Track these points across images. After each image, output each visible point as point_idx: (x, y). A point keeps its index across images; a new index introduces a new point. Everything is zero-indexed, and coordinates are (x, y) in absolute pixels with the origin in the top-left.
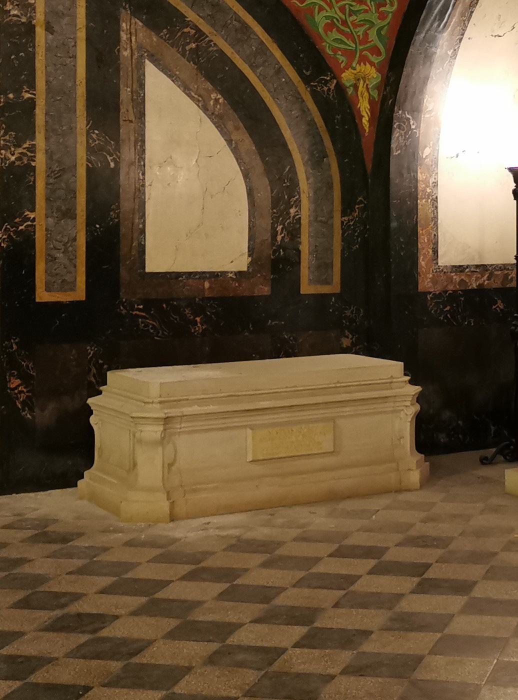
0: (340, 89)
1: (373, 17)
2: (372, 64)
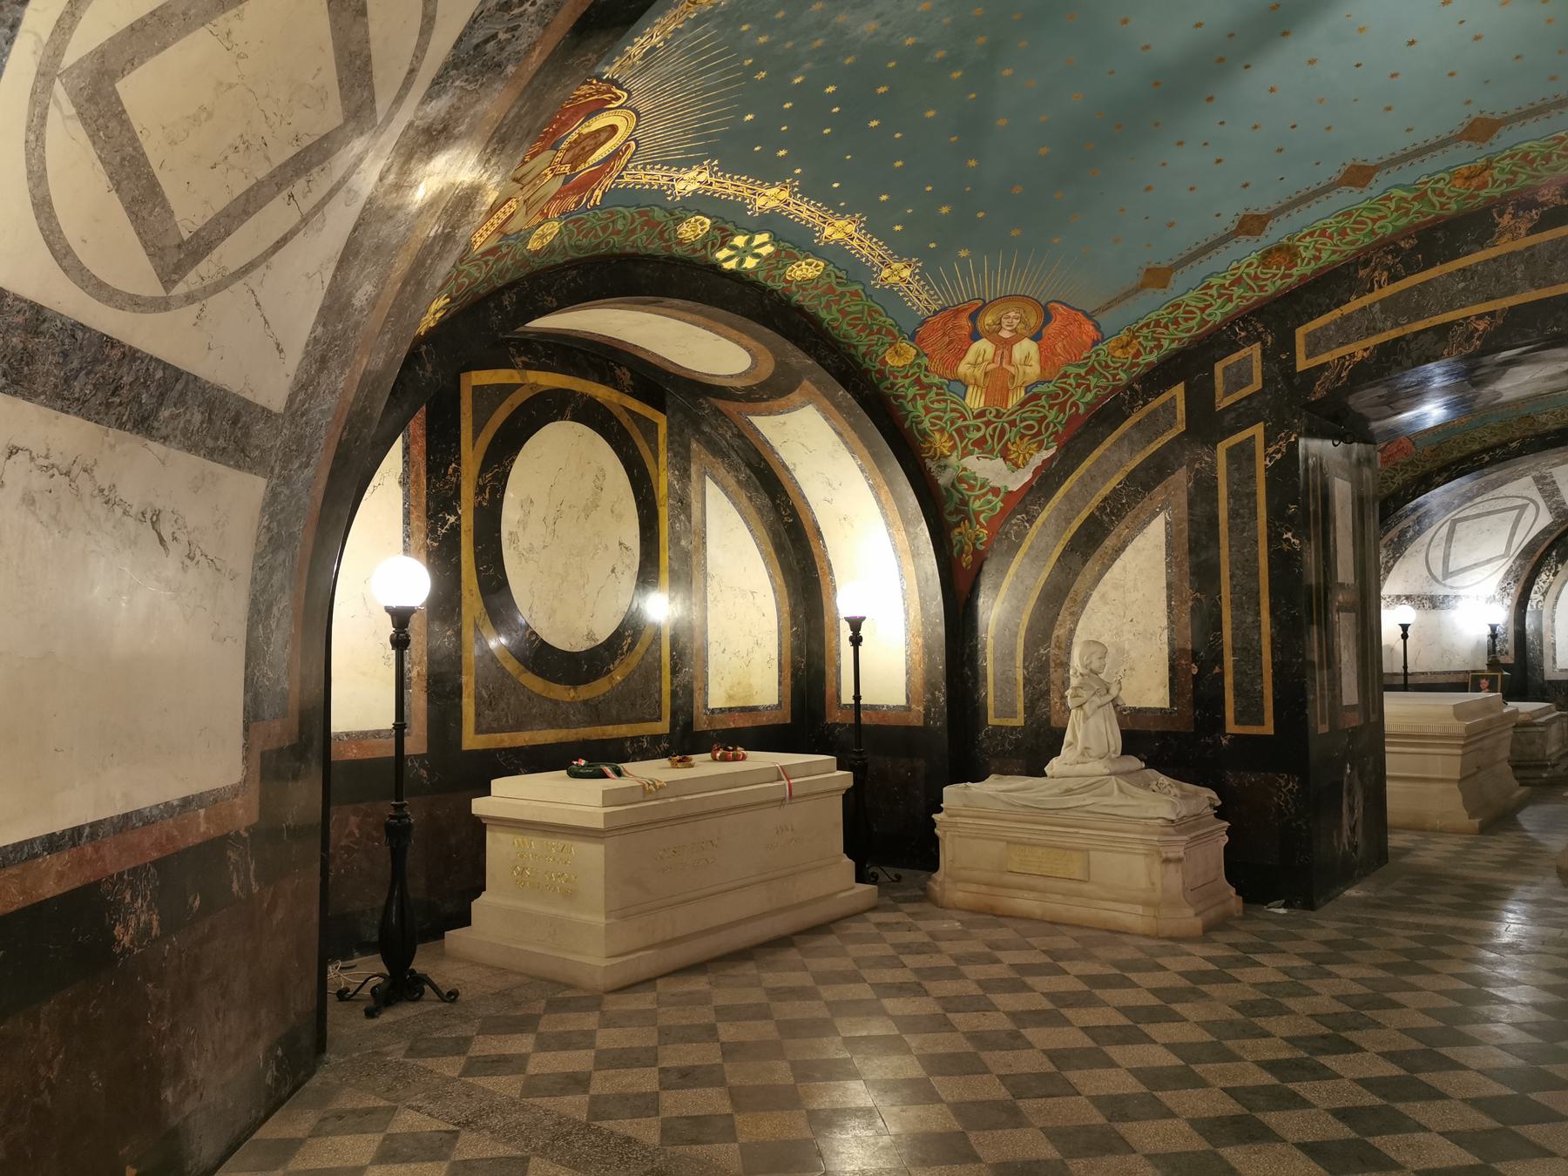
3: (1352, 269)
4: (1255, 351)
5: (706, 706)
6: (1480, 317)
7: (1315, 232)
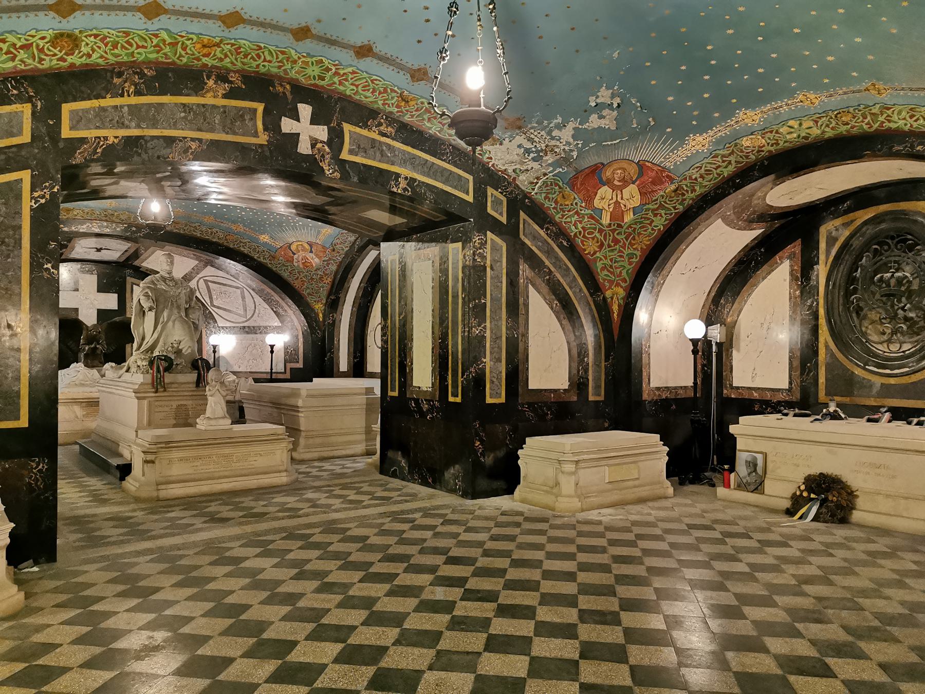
0: (605, 299)
1: (626, 264)
2: (622, 287)
3: (109, 74)
4: (27, 109)
6: (193, 140)
7: (100, 35)
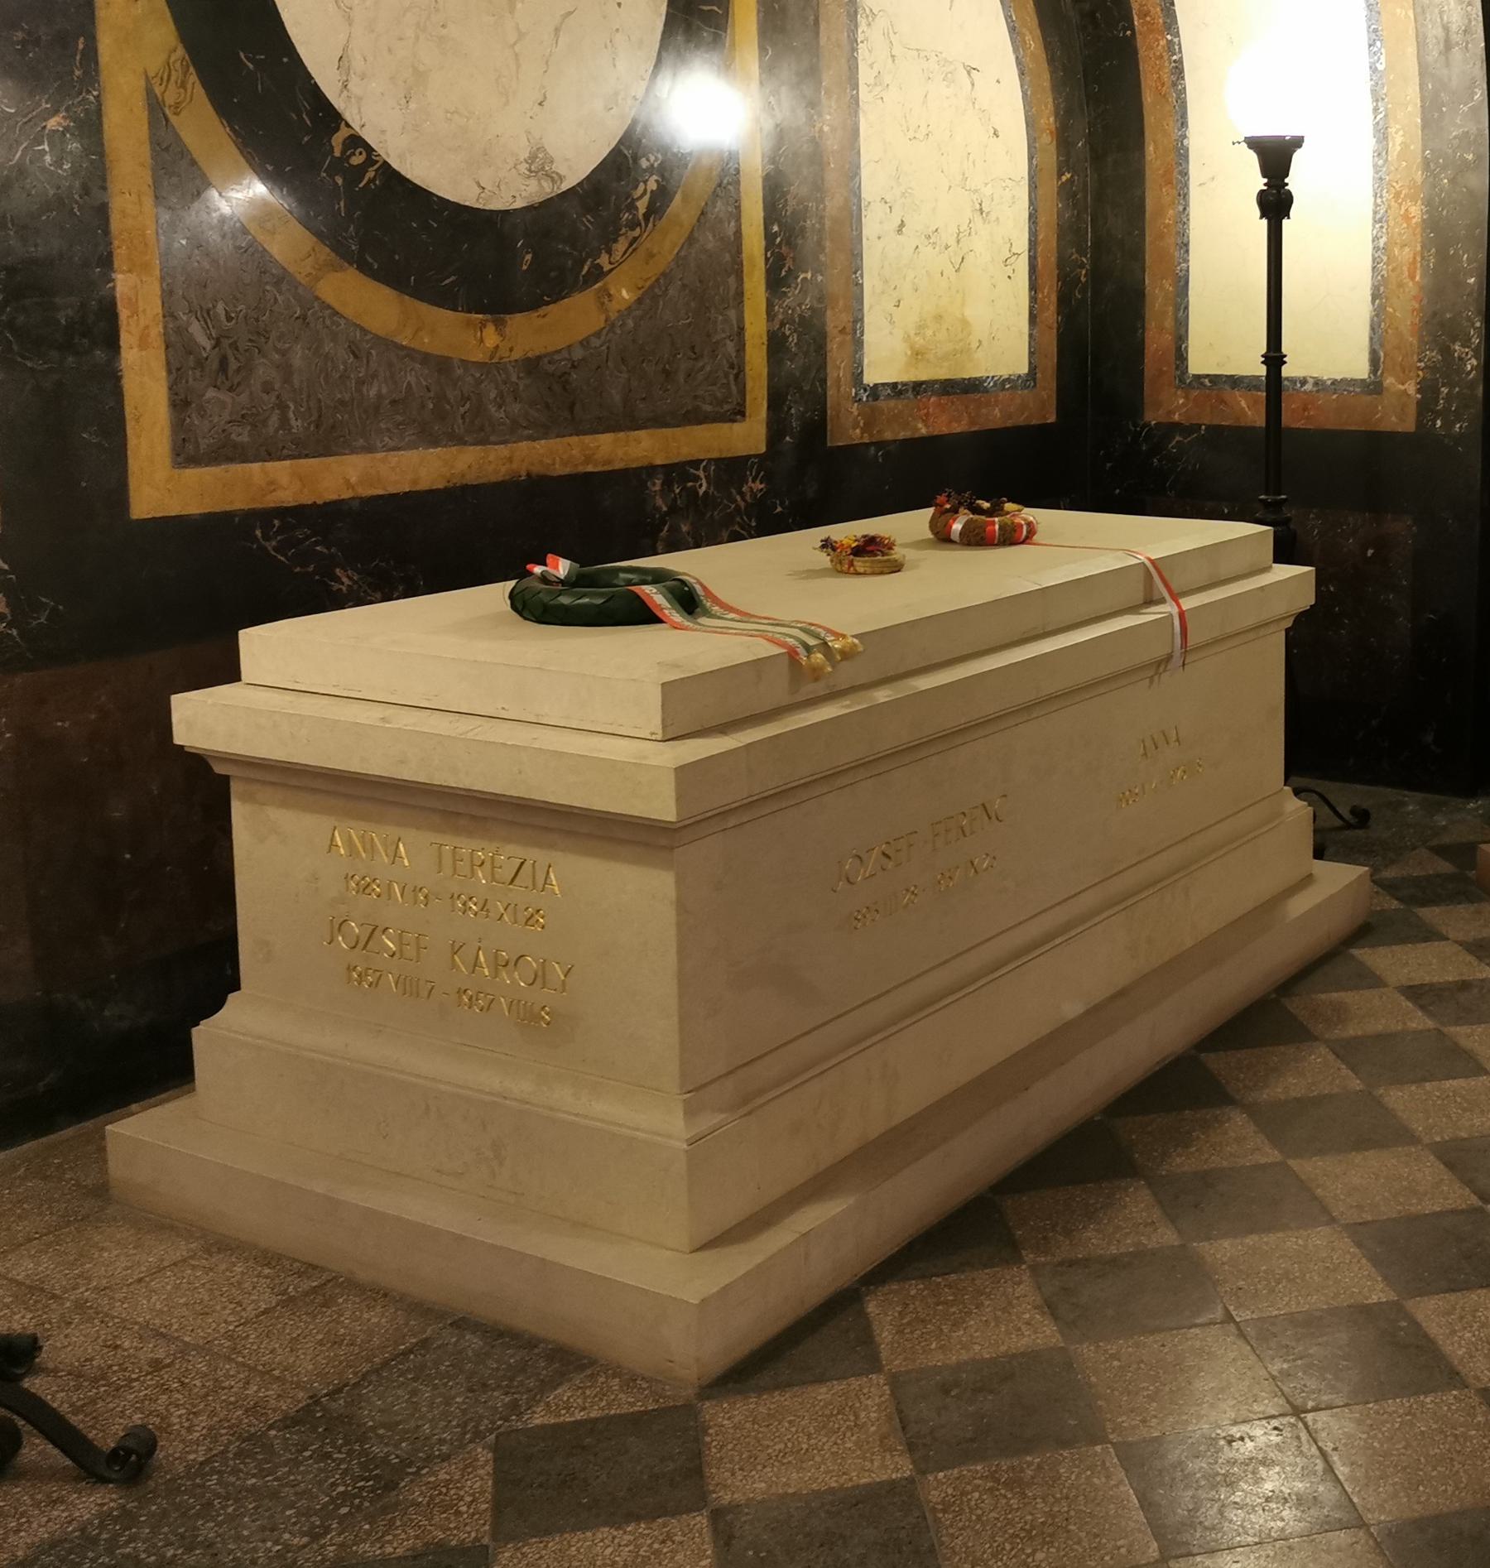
5: (858, 376)
